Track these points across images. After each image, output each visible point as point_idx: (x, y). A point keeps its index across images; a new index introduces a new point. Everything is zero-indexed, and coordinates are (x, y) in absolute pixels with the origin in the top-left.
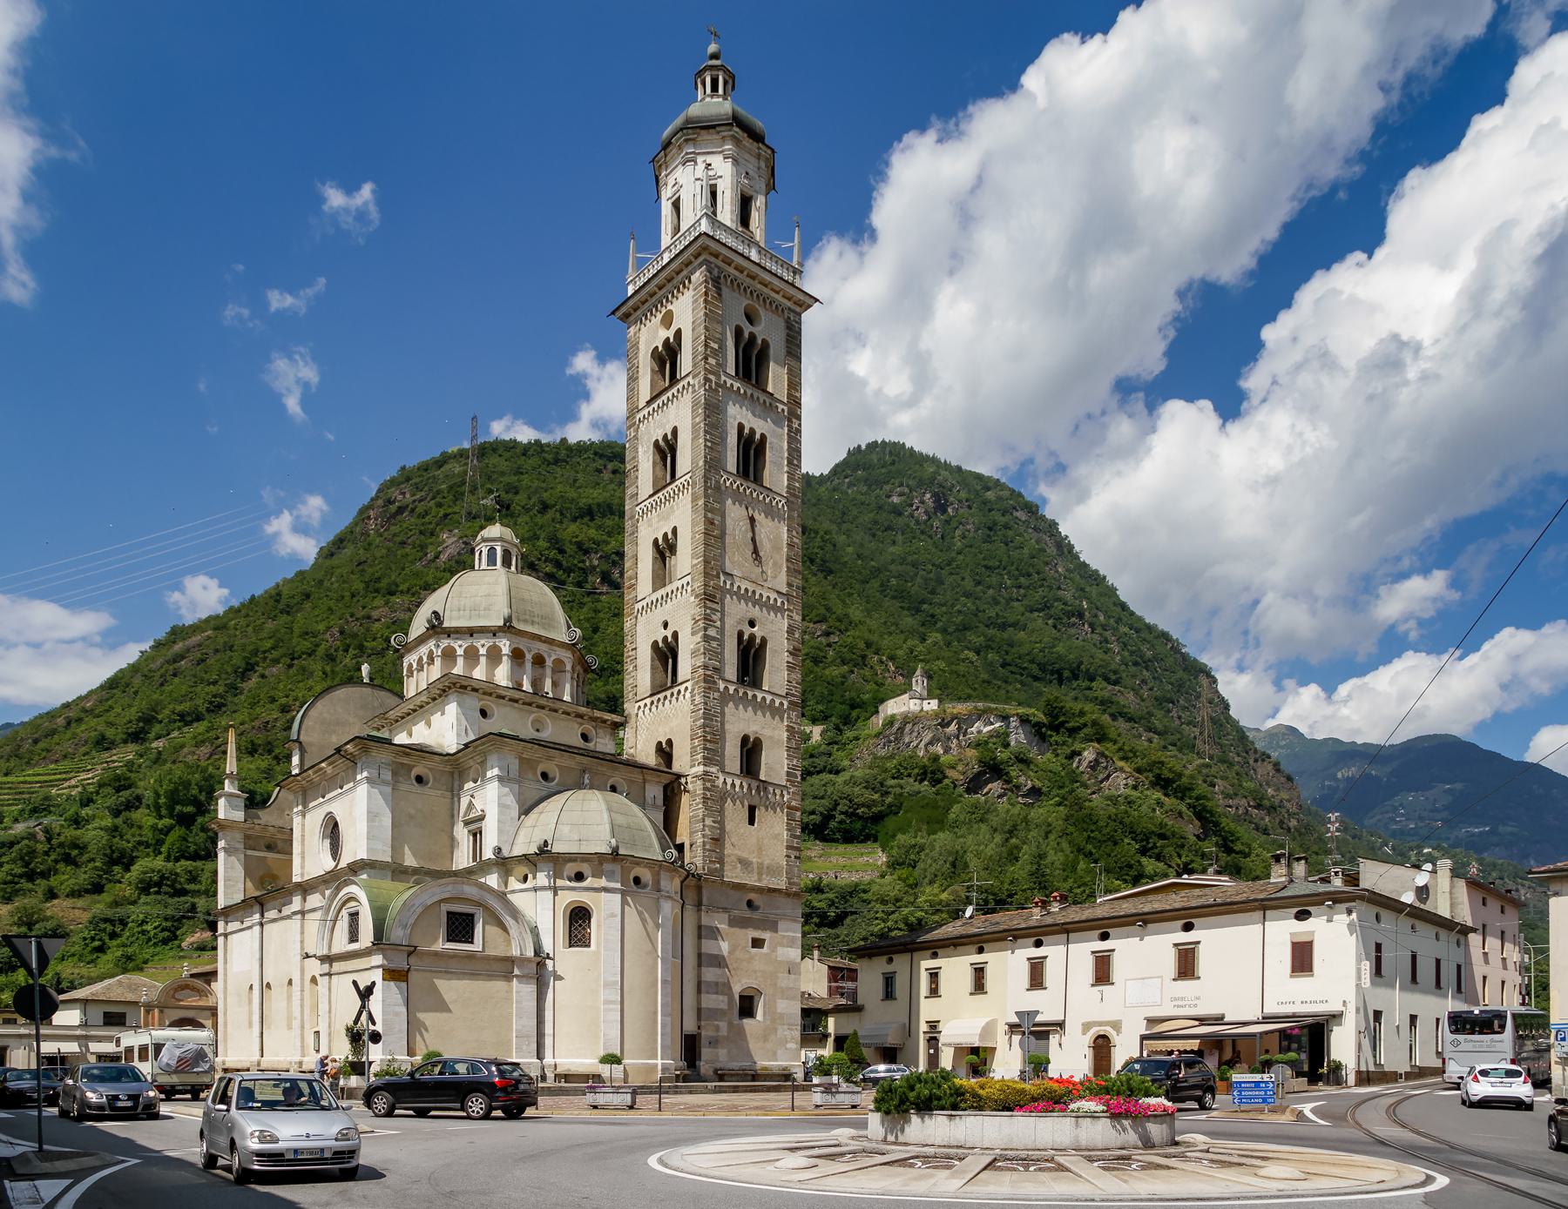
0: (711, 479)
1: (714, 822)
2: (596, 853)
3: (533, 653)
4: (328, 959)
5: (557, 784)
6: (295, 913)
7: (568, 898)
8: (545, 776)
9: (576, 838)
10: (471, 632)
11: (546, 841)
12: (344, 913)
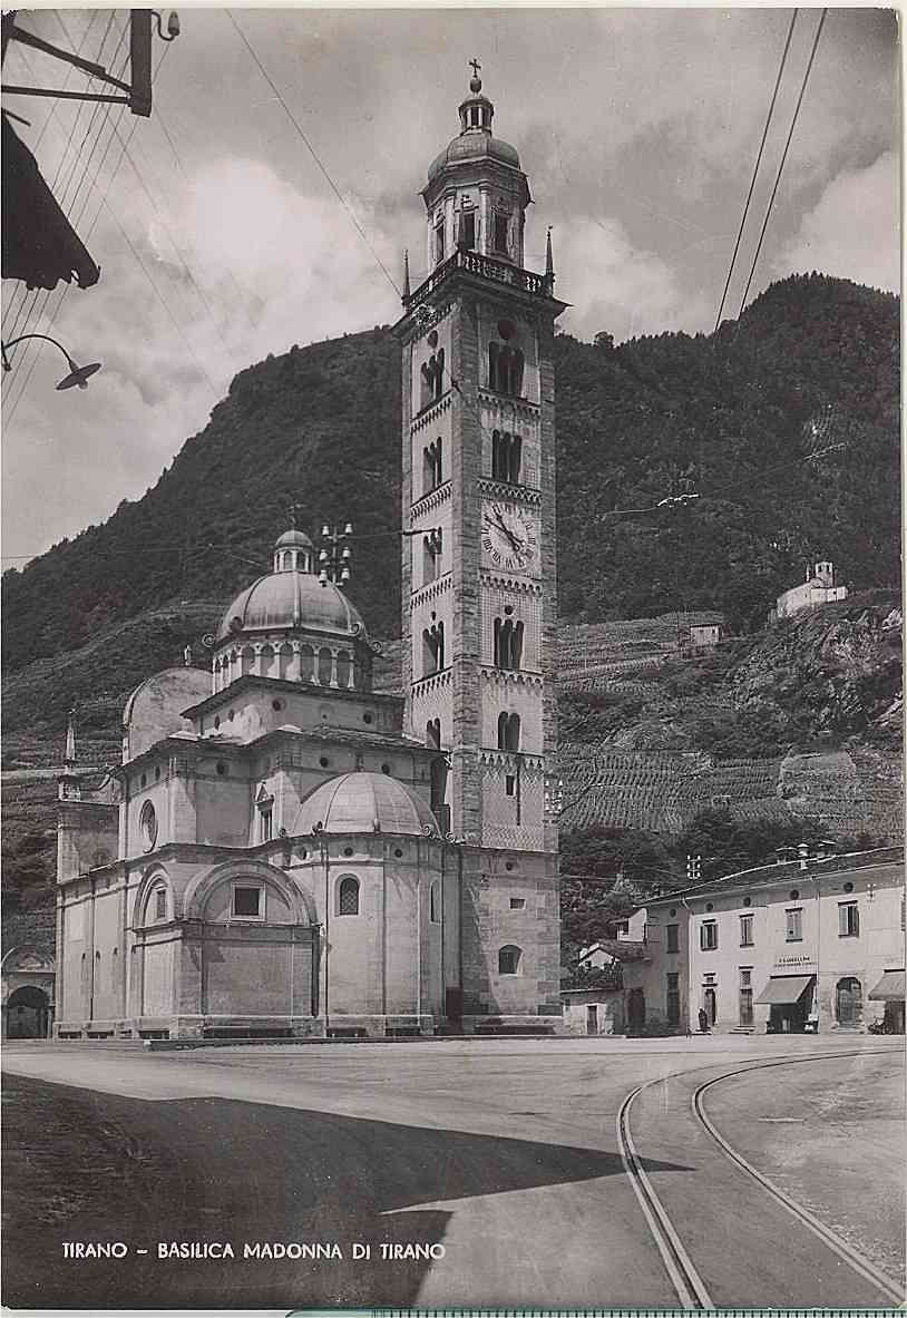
4: (143, 933)
6: (119, 889)
7: (338, 872)
10: (267, 633)
11: (320, 823)
12: (154, 891)
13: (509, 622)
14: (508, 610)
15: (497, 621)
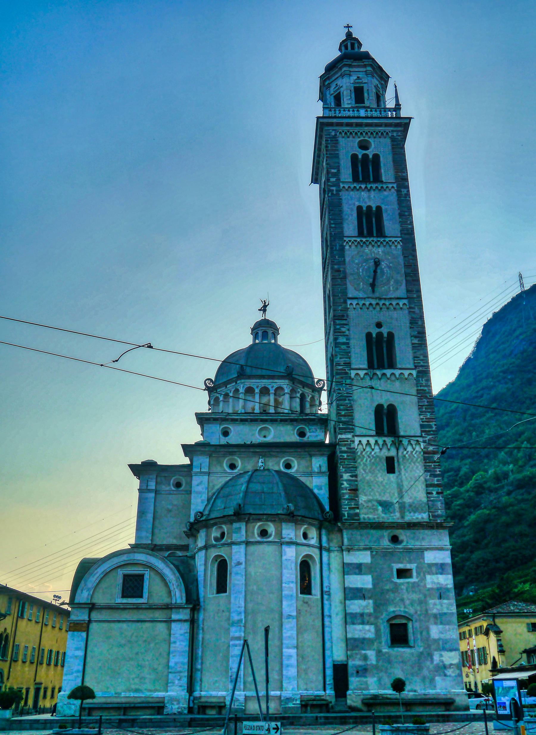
0: (336, 246)
1: (351, 476)
2: (224, 516)
3: (260, 388)
5: (239, 470)
8: (232, 466)
9: (223, 507)
13: (380, 335)
14: (379, 325)
15: (369, 335)
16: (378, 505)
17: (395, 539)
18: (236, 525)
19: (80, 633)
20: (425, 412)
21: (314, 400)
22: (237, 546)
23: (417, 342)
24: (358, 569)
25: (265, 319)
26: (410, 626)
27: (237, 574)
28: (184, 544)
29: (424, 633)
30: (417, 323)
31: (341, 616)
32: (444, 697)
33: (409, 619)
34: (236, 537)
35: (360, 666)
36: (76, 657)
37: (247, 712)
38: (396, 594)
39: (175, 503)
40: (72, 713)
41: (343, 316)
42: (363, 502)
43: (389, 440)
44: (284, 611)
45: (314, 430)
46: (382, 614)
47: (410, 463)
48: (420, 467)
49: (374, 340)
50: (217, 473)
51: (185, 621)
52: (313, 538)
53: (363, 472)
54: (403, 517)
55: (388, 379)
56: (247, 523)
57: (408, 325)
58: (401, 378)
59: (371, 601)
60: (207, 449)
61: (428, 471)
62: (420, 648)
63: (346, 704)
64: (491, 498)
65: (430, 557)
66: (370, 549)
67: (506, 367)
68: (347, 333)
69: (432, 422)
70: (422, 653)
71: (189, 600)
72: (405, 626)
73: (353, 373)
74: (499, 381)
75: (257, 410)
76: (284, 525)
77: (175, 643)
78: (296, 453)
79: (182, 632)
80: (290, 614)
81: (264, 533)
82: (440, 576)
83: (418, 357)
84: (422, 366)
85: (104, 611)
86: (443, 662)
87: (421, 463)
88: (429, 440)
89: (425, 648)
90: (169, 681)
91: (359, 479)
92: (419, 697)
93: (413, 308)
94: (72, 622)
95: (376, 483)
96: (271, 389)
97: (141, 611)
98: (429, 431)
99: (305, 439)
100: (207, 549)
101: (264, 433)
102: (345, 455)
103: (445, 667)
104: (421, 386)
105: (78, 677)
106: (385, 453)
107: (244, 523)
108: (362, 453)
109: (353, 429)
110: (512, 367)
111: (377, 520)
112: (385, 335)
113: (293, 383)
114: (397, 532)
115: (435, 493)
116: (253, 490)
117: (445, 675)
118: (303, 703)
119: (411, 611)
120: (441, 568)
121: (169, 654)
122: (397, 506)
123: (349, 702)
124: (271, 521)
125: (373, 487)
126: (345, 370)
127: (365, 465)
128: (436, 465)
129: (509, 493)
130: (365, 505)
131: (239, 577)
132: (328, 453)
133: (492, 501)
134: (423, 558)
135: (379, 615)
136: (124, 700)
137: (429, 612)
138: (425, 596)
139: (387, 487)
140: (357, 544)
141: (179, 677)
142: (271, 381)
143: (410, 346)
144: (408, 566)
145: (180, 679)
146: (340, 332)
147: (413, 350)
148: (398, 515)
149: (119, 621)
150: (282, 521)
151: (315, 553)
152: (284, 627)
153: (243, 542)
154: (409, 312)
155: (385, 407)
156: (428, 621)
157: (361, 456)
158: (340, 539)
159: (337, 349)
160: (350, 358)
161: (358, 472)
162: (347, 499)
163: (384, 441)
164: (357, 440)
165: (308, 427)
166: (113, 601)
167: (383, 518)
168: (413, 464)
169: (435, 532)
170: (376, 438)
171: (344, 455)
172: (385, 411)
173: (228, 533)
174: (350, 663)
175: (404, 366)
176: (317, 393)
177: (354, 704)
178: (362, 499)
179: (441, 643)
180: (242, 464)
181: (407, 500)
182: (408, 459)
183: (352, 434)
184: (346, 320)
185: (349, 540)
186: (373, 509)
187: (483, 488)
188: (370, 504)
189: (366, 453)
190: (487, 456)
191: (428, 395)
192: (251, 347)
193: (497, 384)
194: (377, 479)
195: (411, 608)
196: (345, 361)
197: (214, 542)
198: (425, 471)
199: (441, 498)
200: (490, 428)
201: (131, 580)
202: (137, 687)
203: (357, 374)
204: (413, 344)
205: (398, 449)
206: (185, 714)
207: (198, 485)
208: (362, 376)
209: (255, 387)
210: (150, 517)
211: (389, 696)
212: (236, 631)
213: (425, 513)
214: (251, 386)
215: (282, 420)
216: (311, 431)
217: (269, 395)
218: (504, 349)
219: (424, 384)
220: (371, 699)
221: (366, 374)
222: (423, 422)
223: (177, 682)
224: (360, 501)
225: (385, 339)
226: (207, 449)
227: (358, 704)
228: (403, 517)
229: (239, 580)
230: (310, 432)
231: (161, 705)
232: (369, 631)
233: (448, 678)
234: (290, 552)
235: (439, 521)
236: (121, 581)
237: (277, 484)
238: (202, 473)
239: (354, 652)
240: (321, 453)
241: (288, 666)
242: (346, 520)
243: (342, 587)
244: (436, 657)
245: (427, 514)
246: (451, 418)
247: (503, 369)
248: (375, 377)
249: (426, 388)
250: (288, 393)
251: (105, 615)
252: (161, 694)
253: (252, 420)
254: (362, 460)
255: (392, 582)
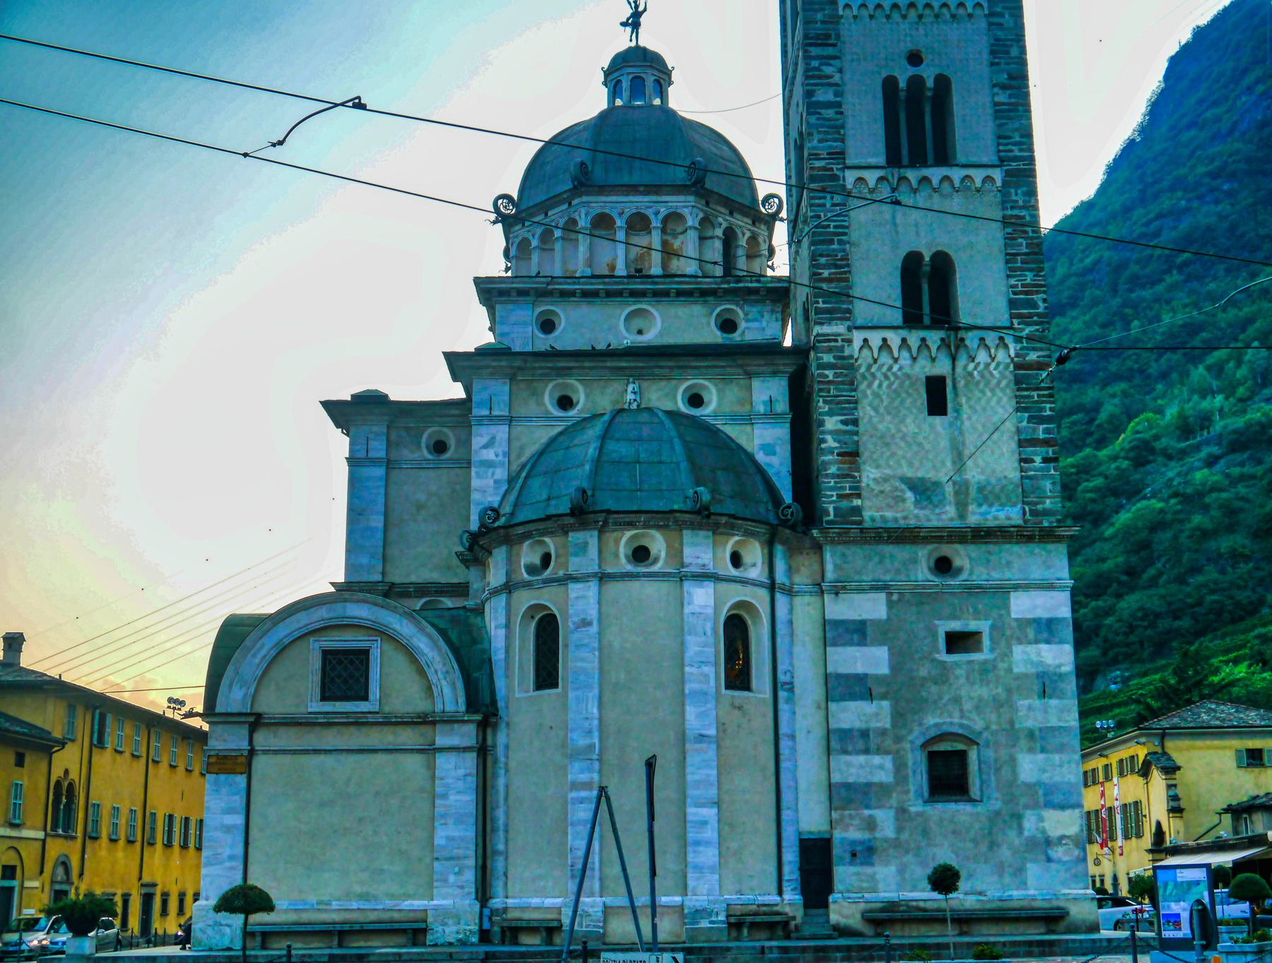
1: (843, 422)
2: (548, 518)
3: (626, 216)
8: (565, 402)
9: (544, 496)
13: (916, 82)
14: (915, 58)
15: (889, 84)
16: (903, 487)
17: (943, 566)
18: (575, 537)
19: (232, 776)
20: (1022, 269)
21: (758, 244)
22: (579, 586)
23: (1006, 100)
24: (857, 632)
25: (637, 47)
26: (973, 755)
27: (578, 647)
28: (455, 581)
29: (1006, 772)
30: (1008, 53)
31: (819, 732)
32: (1045, 905)
33: (972, 742)
34: (575, 564)
35: (861, 843)
36: (228, 829)
37: (608, 940)
38: (945, 688)
39: (434, 488)
40: (226, 943)
41: (828, 36)
42: (871, 483)
43: (934, 337)
44: (688, 726)
45: (758, 316)
46: (911, 731)
47: (983, 392)
48: (1005, 399)
49: (903, 95)
50: (528, 418)
51: (466, 749)
52: (754, 565)
53: (872, 413)
54: (962, 516)
55: (935, 190)
56: (601, 532)
57: (986, 56)
58: (968, 188)
59: (886, 704)
60: (503, 363)
61: (1025, 410)
62: (995, 803)
63: (828, 921)
64: (1171, 474)
65: (1022, 605)
66: (884, 588)
67: (1217, 163)
68: (837, 78)
69: (1037, 293)
70: (998, 814)
71: (472, 703)
72: (962, 755)
73: (850, 177)
74: (1201, 198)
75: (621, 270)
76: (687, 535)
77: (445, 796)
78: (718, 370)
79: (461, 772)
80: (704, 732)
81: (641, 554)
82: (1044, 647)
83: (1010, 138)
84: (1016, 159)
85: (282, 731)
86: (1044, 832)
87: (1008, 391)
88: (1029, 338)
89: (1006, 803)
90: (435, 877)
91: (861, 429)
92: (988, 906)
93: (1001, 15)
94: (212, 753)
95: (903, 438)
96: (652, 217)
97: (364, 729)
98: (1030, 316)
99: (736, 337)
100: (510, 592)
101: (638, 323)
102: (830, 374)
103: (1048, 842)
104: (1012, 208)
105: (232, 868)
106: (925, 368)
107: (596, 533)
108: (869, 367)
109: (849, 311)
110: (1234, 162)
111: (902, 523)
112: (930, 83)
113: (707, 204)
114: (946, 550)
115: (1038, 459)
116: (614, 455)
117: (1049, 860)
118: (732, 920)
119: (979, 725)
120: (1045, 629)
121: (433, 819)
122: (949, 489)
123: (834, 918)
124: (658, 527)
125: (894, 448)
126: (832, 169)
127: (876, 395)
128: (1044, 396)
129: (1211, 462)
130: (877, 488)
131: (583, 653)
132: (790, 369)
133: (1171, 480)
134: (1007, 608)
135: (904, 732)
136: (336, 917)
137: (1017, 726)
138: (1009, 691)
139: (928, 447)
140: (856, 578)
141: (457, 869)
142: (654, 198)
143: (990, 111)
144: (973, 626)
145: (459, 873)
146: (820, 77)
147: (996, 118)
148: (951, 511)
149: (317, 751)
150: (681, 526)
151: (759, 597)
152: (689, 760)
153: (594, 575)
154: (990, 24)
155: (927, 259)
156: (1014, 746)
157: (867, 375)
158: (816, 567)
159: (813, 119)
160: (843, 141)
161: (860, 413)
162: (834, 476)
163: (923, 340)
164: (858, 337)
165: (742, 308)
166: (303, 710)
167: (917, 517)
168: (989, 394)
169: (1036, 548)
170: (904, 333)
171: (827, 372)
172: (927, 269)
173: (557, 556)
174: (838, 835)
175: (973, 160)
176: (762, 227)
177: (843, 921)
178: (869, 474)
179: (1041, 792)
180: (587, 396)
181: (973, 475)
182: (978, 384)
183: (848, 323)
184: (834, 45)
185: (837, 567)
186: (895, 498)
187: (1152, 451)
188: (887, 487)
189: (879, 368)
190: (1164, 376)
191: (1029, 229)
192: (603, 116)
193: (1195, 204)
194: (904, 429)
195: (974, 716)
196: (830, 147)
197: (525, 575)
198: (1017, 410)
199: (1052, 472)
200: (1174, 311)
201: (340, 662)
202: (365, 889)
203: (860, 180)
204: (996, 104)
205: (954, 359)
206: (473, 944)
207: (485, 447)
208: (872, 184)
209: (614, 214)
210: (377, 522)
211: (922, 904)
212: (582, 772)
213: (1014, 505)
214: (607, 211)
215: (680, 293)
216: (750, 317)
217: (650, 233)
218: (1218, 119)
219: (1021, 203)
220: (882, 910)
221: (881, 179)
222: (1015, 293)
223: (452, 878)
224: (865, 480)
225: (929, 94)
226: (503, 363)
227: (855, 922)
228: (962, 516)
229: (583, 660)
230: (747, 321)
231: (423, 926)
232: (881, 767)
233: (1053, 865)
234: (702, 597)
235: (1046, 524)
236: (316, 663)
237: (671, 440)
238: (492, 420)
239: (847, 812)
240: (773, 368)
241: (697, 843)
242: (829, 522)
243: (822, 671)
244: (1030, 824)
245: (1019, 506)
246: (1082, 287)
247: (1211, 167)
248: (903, 188)
249: (1023, 213)
250: (696, 228)
251: (286, 738)
252: (418, 904)
253: (609, 294)
254: (870, 385)
255: (934, 660)
